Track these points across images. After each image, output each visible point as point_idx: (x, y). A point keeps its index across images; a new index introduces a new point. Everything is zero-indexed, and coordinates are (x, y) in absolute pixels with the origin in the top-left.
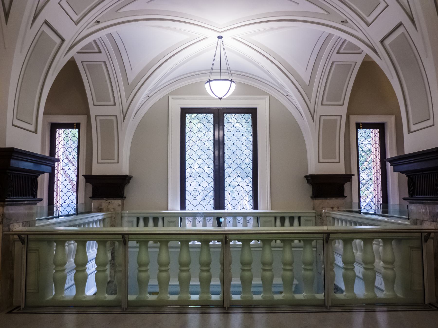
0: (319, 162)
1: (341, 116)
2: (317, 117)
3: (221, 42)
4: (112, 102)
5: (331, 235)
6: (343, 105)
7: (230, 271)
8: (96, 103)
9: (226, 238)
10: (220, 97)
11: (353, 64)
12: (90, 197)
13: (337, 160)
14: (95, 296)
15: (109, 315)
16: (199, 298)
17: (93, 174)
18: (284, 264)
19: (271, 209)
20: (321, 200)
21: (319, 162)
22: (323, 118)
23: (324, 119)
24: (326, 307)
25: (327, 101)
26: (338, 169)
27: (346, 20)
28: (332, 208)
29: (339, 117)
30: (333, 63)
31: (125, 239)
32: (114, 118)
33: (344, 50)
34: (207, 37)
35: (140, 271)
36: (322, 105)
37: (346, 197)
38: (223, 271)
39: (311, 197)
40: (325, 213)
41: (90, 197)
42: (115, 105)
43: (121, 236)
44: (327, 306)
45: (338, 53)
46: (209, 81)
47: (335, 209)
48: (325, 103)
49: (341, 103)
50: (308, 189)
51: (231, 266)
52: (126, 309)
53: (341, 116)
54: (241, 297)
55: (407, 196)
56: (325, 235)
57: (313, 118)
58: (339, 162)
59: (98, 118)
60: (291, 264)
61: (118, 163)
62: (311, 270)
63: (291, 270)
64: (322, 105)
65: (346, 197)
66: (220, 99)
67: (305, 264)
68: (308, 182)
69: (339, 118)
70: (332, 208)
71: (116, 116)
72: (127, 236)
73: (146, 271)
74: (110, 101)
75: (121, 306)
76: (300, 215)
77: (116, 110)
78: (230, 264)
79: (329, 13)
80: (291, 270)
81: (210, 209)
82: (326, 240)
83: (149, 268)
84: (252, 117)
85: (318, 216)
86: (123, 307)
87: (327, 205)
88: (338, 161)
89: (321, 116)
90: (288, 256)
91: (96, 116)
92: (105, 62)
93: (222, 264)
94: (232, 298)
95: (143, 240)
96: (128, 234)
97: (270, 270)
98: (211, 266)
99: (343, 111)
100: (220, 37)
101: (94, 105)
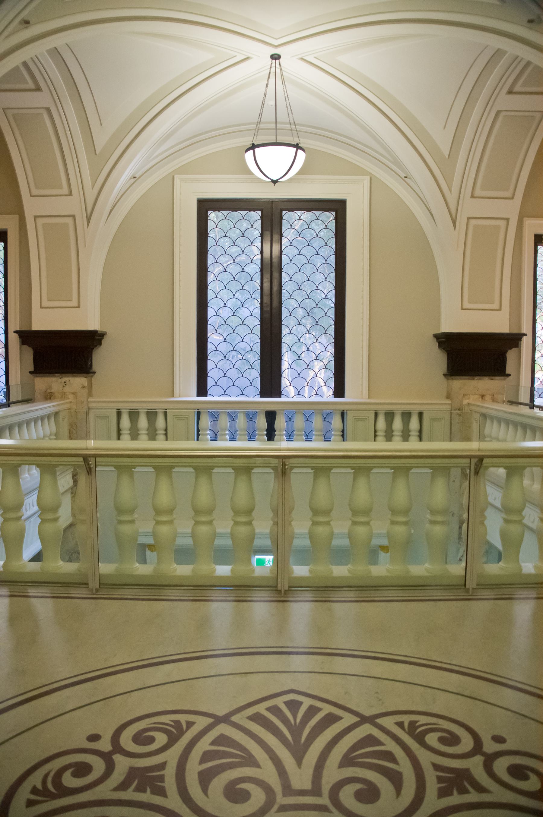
0: (462, 309)
1: (508, 219)
3: (278, 66)
4: (65, 191)
5: (485, 461)
6: (512, 198)
7: (290, 524)
8: (35, 192)
9: (284, 464)
12: (30, 372)
13: (496, 306)
14: (39, 564)
15: (67, 600)
16: (232, 571)
17: (33, 329)
18: (394, 512)
19: (368, 398)
21: (462, 309)
22: (473, 222)
23: (475, 226)
24: (467, 590)
26: (496, 323)
28: (483, 396)
31: (88, 464)
32: (70, 221)
34: (250, 55)
35: (121, 522)
36: (472, 196)
37: (509, 375)
38: (276, 523)
39: (445, 375)
40: (469, 404)
41: (30, 372)
42: (70, 194)
43: (81, 459)
44: (469, 589)
46: (253, 147)
47: (488, 398)
48: (478, 193)
49: (508, 194)
50: (439, 360)
51: (293, 514)
52: (97, 590)
53: (508, 219)
54: (310, 571)
56: (474, 461)
57: (454, 222)
59: (40, 221)
60: (406, 512)
61: (79, 307)
62: (443, 523)
63: (405, 523)
64: (472, 196)
65: (509, 375)
66: (275, 182)
67: (433, 512)
68: (440, 346)
69: (503, 223)
70: (483, 396)
71: (73, 216)
72: (93, 459)
73: (132, 522)
74: (61, 187)
75: (87, 584)
76: (421, 408)
77: (72, 205)
78: (290, 512)
80: (405, 523)
81: (253, 396)
82: (475, 469)
83: (136, 516)
84: (336, 218)
85: (455, 410)
86: (90, 585)
87: (475, 390)
89: (469, 218)
90: (401, 495)
91: (36, 217)
92: (48, 110)
93: (276, 512)
94: (292, 572)
95: (125, 464)
96: (95, 456)
97: (367, 523)
98: (253, 514)
99: (512, 209)
101: (31, 196)
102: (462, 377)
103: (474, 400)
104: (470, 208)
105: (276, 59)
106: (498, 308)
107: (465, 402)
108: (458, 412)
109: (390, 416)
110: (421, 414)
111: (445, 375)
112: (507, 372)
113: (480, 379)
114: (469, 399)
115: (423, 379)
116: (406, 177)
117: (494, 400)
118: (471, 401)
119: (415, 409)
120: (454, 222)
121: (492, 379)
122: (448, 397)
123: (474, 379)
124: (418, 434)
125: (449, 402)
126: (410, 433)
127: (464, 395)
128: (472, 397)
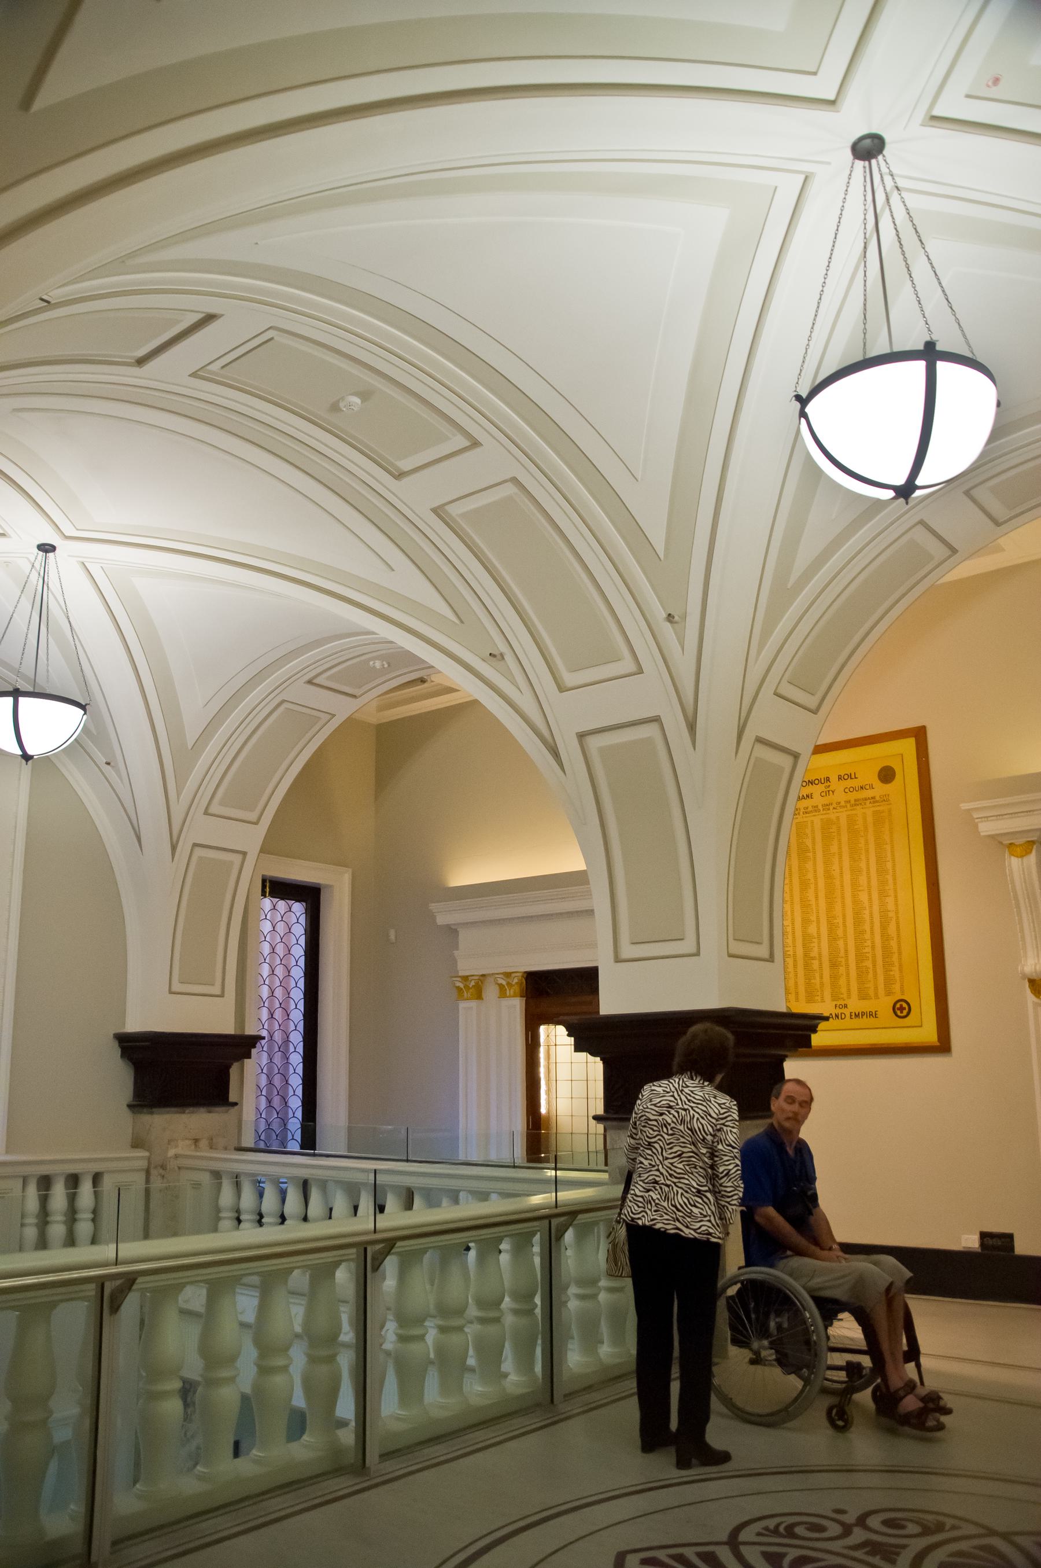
0: (171, 992)
1: (244, 854)
2: (184, 848)
6: (256, 823)
10: (30, 752)
11: (325, 717)
19: (7, 1152)
20: (167, 1117)
22: (199, 852)
23: (200, 858)
25: (222, 803)
26: (212, 1017)
27: (502, 655)
28: (196, 1141)
29: (240, 857)
30: (283, 701)
33: (328, 678)
34: (9, 531)
36: (206, 813)
37: (236, 1104)
39: (129, 1106)
40: (176, 1156)
45: (310, 682)
48: (213, 809)
49: (253, 816)
53: (244, 854)
55: (600, 1111)
57: (174, 848)
58: (222, 996)
64: (206, 813)
66: (26, 757)
68: (123, 1056)
69: (237, 859)
70: (196, 1141)
79: (462, 622)
85: (156, 1167)
88: (219, 992)
89: (195, 845)
99: (252, 839)
100: (47, 548)
102: (168, 1109)
103: (183, 1148)
104: (202, 829)
105: (46, 551)
106: (174, 989)
107: (171, 1152)
108: (161, 1171)
109: (45, 1183)
110: (97, 1178)
111: (130, 1106)
112: (233, 1097)
113: (193, 1112)
114: (177, 1146)
115: (94, 1117)
116: (108, 764)
117: (212, 1147)
118: (179, 1151)
119: (87, 1169)
120: (174, 848)
121: (210, 1112)
122: (137, 1143)
123: (184, 1113)
124: (91, 1216)
125: (147, 1154)
126: (49, 1219)
127: (169, 1142)
128: (181, 1143)
